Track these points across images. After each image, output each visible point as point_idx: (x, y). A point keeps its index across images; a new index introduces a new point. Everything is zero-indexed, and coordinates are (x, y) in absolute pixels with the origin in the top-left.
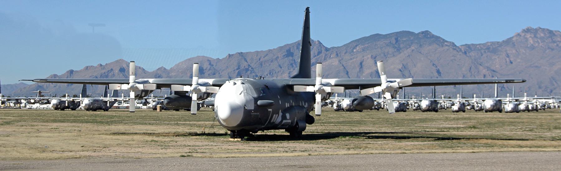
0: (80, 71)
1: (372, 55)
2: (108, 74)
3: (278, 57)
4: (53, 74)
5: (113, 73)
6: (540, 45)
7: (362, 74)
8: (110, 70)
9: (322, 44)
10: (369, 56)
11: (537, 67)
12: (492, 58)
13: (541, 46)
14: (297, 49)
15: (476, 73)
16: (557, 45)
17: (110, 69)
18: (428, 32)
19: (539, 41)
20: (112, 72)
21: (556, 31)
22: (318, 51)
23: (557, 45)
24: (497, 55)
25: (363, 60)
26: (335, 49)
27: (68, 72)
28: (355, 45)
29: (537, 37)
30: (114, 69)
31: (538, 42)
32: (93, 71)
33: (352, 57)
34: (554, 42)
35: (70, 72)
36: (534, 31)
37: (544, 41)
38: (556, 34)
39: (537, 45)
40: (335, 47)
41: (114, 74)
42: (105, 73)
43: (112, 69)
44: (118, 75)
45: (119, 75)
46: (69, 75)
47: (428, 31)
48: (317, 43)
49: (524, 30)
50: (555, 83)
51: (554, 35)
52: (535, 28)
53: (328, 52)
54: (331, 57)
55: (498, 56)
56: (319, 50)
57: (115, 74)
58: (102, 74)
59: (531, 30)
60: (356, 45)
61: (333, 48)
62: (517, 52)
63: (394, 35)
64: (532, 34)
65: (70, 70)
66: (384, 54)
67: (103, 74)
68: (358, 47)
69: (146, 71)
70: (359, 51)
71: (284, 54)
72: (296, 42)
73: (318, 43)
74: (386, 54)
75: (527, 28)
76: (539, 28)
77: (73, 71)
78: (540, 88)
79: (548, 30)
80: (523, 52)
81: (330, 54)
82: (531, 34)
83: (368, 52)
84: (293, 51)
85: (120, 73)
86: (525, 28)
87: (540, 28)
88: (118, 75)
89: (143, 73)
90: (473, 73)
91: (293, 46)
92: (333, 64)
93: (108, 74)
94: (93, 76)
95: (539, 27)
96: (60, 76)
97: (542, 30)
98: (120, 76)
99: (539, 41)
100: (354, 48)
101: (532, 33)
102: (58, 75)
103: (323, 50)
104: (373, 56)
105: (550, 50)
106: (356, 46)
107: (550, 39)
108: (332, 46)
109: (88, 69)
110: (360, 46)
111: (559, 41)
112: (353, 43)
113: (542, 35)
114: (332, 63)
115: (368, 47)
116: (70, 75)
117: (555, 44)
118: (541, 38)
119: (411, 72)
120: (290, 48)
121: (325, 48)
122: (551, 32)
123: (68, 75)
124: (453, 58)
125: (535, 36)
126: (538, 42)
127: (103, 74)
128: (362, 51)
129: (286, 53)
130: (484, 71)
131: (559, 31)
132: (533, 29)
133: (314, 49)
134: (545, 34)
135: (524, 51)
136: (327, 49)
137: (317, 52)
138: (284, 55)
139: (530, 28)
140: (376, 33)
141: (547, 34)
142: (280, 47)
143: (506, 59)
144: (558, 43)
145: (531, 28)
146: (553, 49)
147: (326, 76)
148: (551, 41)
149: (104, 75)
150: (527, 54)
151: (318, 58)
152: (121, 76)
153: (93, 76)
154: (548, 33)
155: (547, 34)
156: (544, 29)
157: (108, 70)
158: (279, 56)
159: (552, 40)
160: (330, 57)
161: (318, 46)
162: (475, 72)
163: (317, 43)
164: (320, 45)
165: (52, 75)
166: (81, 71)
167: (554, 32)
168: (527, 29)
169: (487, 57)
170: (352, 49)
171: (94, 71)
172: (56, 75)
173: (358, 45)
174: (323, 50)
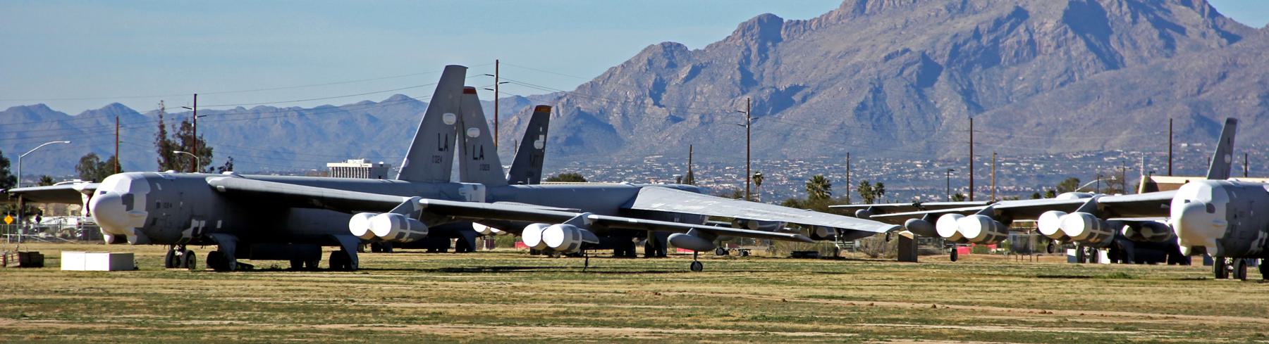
0: (820, 20)
2: (996, 41)
4: (657, 42)
5: (1025, 38)
8: (1009, 18)
17: (1008, 9)
20: (1022, 29)
27: (745, 29)
30: (1031, 9)
32: (900, 22)
35: (756, 30)
41: (1031, 42)
42: (977, 34)
43: (1020, 15)
44: (1058, 47)
45: (1062, 50)
46: (754, 49)
57: (1036, 37)
58: (961, 40)
65: (760, 19)
67: (965, 43)
69: (1225, 21)
77: (782, 19)
85: (1070, 34)
88: (1058, 47)
89: (1212, 31)
93: (996, 41)
94: (908, 54)
96: (697, 51)
98: (1067, 52)
102: (691, 49)
109: (867, 12)
116: (763, 51)
123: (749, 49)
127: (965, 43)
149: (974, 43)
152: (1074, 54)
153: (906, 50)
157: (994, 13)
165: (650, 47)
166: (822, 23)
171: (905, 26)
172: (679, 45)
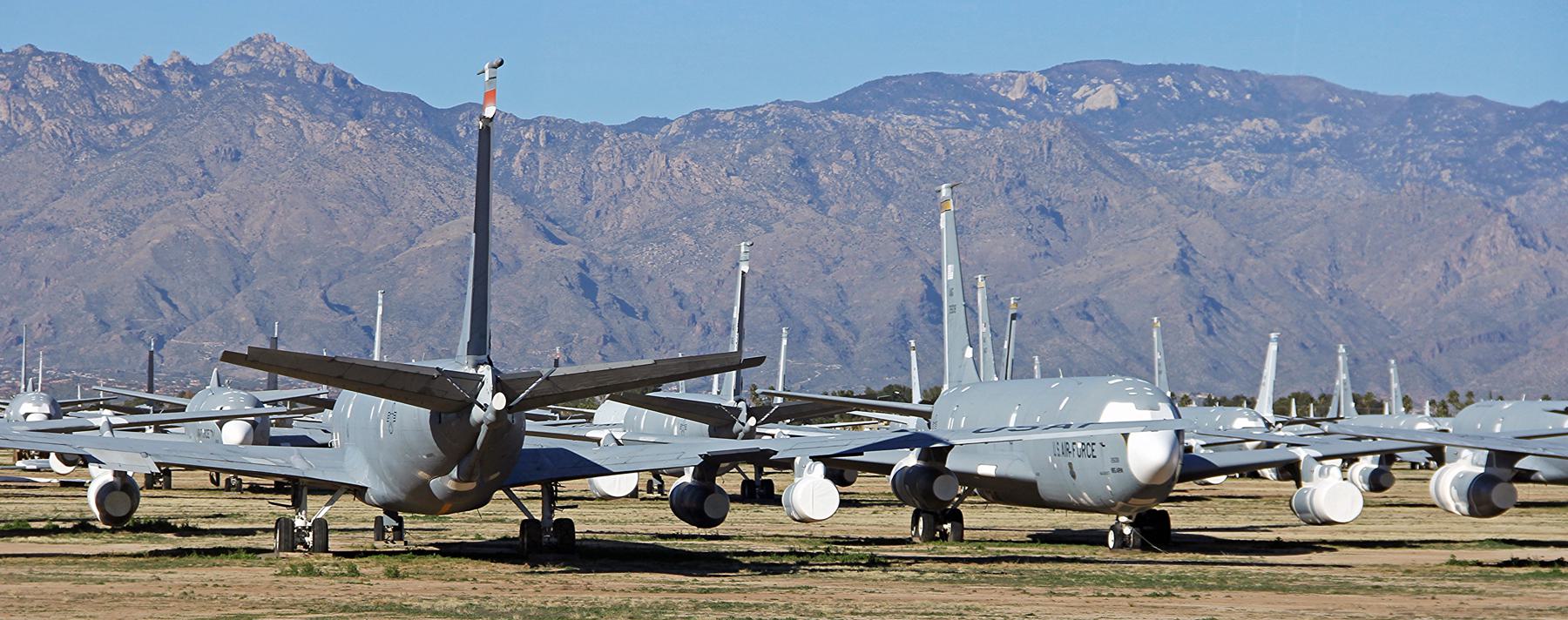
6: (48, 126)
13: (54, 135)
16: (123, 131)
19: (39, 109)
23: (123, 131)
29: (26, 92)
31: (29, 113)
34: (107, 118)
37: (62, 112)
39: (28, 125)
50: (162, 304)
51: (103, 84)
76: (29, 50)
78: (105, 325)
79: (73, 60)
87: (37, 52)
95: (32, 46)
97: (46, 61)
99: (39, 109)
107: (87, 102)
111: (126, 115)
113: (49, 82)
117: (113, 127)
118: (45, 96)
122: (86, 71)
125: (15, 87)
126: (29, 113)
134: (59, 78)
141: (69, 77)
144: (126, 122)
146: (104, 152)
148: (91, 112)
154: (73, 75)
155: (69, 77)
156: (55, 57)
159: (98, 107)
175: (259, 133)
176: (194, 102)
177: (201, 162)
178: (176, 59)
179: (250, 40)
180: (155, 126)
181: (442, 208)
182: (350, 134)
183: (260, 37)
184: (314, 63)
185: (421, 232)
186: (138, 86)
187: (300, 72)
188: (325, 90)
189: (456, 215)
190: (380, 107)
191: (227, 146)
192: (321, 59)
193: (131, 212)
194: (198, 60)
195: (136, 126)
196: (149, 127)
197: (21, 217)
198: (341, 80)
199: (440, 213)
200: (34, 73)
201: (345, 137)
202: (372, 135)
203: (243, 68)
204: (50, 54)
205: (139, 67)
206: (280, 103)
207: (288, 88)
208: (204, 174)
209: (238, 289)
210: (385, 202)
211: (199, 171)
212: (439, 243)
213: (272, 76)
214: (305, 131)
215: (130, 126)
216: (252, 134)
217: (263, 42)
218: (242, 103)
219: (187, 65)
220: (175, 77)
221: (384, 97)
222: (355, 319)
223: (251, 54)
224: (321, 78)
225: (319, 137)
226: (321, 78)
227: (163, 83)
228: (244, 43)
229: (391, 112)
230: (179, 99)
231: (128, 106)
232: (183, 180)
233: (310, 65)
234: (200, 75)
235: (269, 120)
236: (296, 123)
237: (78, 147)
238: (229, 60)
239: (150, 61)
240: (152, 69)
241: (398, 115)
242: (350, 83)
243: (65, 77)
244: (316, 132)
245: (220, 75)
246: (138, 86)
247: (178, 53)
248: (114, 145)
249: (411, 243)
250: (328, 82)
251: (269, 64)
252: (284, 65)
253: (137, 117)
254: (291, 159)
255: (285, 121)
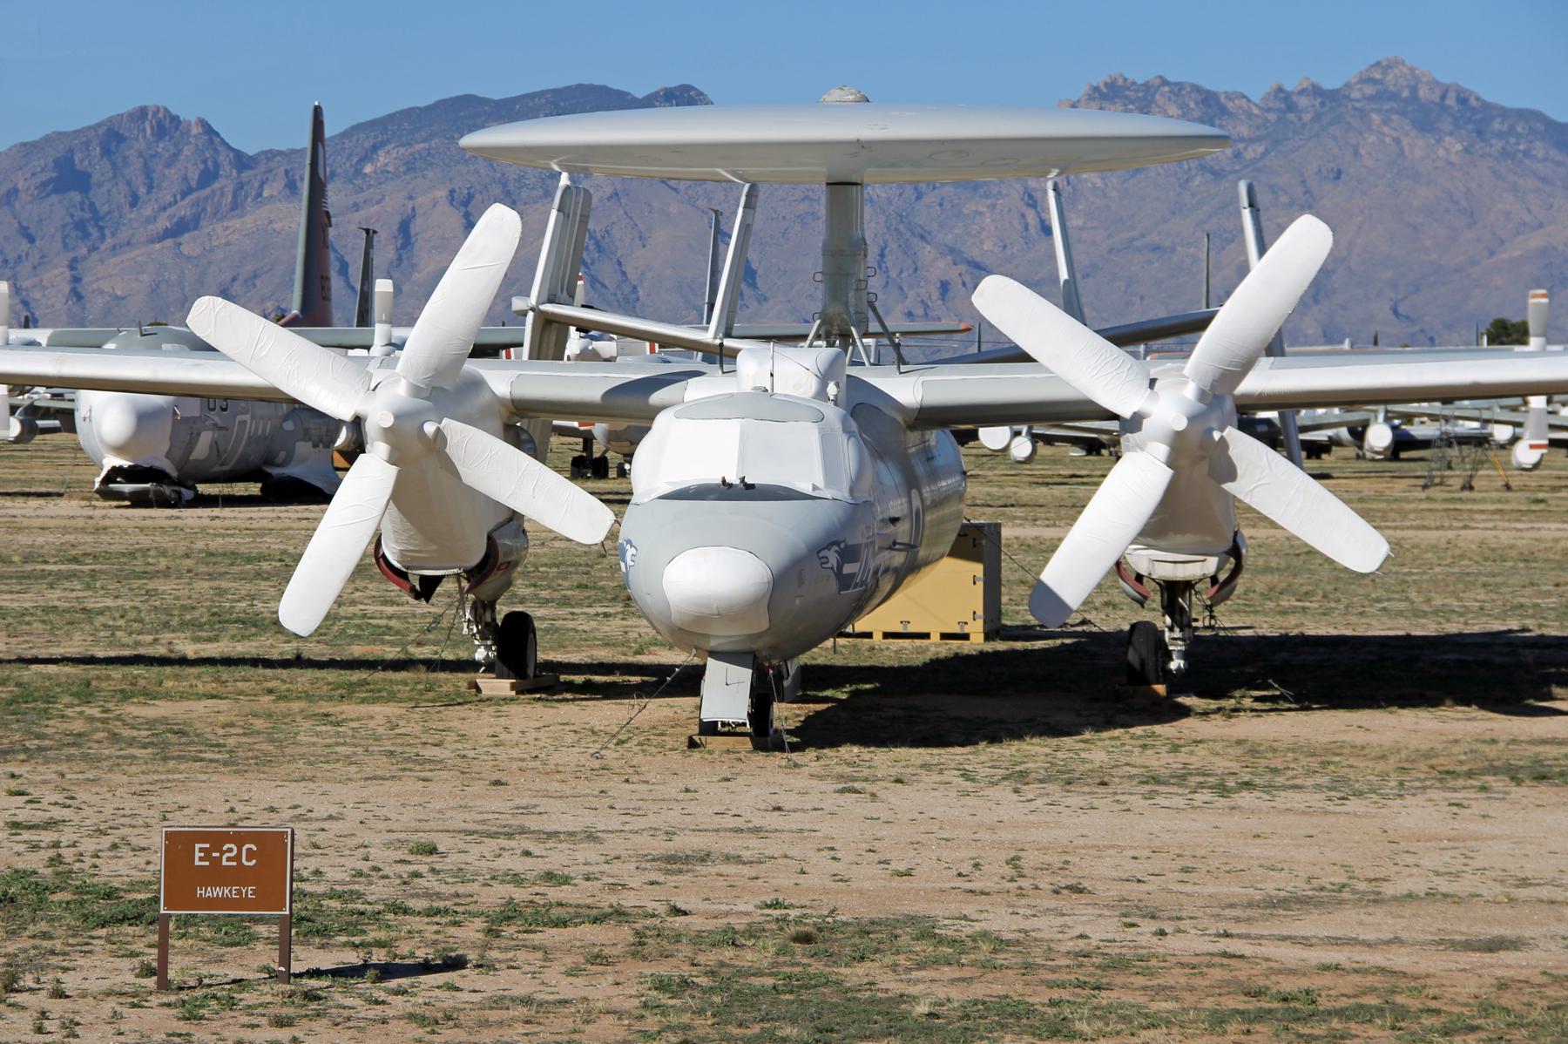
1: (452, 192)
3: (14, 192)
7: (411, 274)
9: (217, 134)
10: (441, 194)
11: (1156, 248)
12: (965, 211)
14: (102, 155)
15: (904, 275)
16: (1237, 155)
18: (692, 93)
21: (1229, 96)
22: (202, 167)
23: (1237, 155)
24: (987, 196)
25: (413, 209)
26: (278, 158)
28: (367, 145)
33: (360, 198)
36: (1140, 94)
38: (1230, 105)
40: (280, 153)
47: (693, 88)
48: (195, 130)
49: (1096, 89)
51: (1223, 110)
52: (1140, 81)
53: (246, 175)
54: (266, 193)
55: (989, 202)
56: (205, 162)
59: (1128, 89)
60: (372, 142)
61: (270, 155)
62: (1069, 184)
63: (543, 101)
64: (1131, 107)
66: (505, 185)
68: (380, 152)
70: (391, 168)
71: (44, 177)
72: (99, 125)
73: (200, 130)
74: (511, 187)
75: (1108, 81)
76: (1158, 82)
79: (1197, 89)
80: (1094, 184)
81: (256, 185)
82: (1125, 105)
83: (430, 174)
84: (86, 162)
86: (1100, 79)
87: (1165, 82)
90: (893, 274)
91: (87, 144)
92: (277, 226)
95: (1161, 77)
100: (367, 157)
101: (1132, 102)
103: (224, 159)
104: (456, 196)
105: (1209, 176)
106: (375, 149)
108: (266, 148)
110: (389, 147)
111: (1242, 140)
112: (362, 136)
114: (271, 222)
115: (429, 154)
117: (1229, 152)
119: (628, 268)
120: (71, 150)
121: (231, 155)
124: (804, 207)
128: (405, 173)
129: (54, 175)
130: (941, 264)
131: (1244, 96)
132: (1134, 83)
133: (182, 157)
135: (1099, 183)
136: (242, 161)
137: (198, 172)
138: (44, 184)
139: (1120, 82)
140: (597, 82)
141: (1192, 105)
142: (24, 145)
143: (1023, 216)
144: (1241, 146)
145: (1125, 80)
147: (246, 281)
150: (1114, 194)
151: (207, 198)
154: (1196, 103)
155: (1192, 105)
156: (1180, 86)
158: (20, 187)
160: (260, 195)
161: (200, 143)
162: (901, 272)
163: (195, 130)
164: (211, 142)
167: (1223, 100)
168: (1106, 84)
169: (941, 205)
170: (355, 160)
173: (382, 144)
174: (224, 159)
175: (1362, 151)
176: (1304, 126)
177: (1303, 182)
178: (1305, 85)
179: (1378, 64)
180: (1266, 149)
181: (1528, 218)
182: (1446, 149)
183: (1388, 60)
184: (1437, 83)
185: (1502, 242)
186: (1256, 111)
187: (1423, 92)
188: (1443, 108)
189: (1541, 226)
190: (1502, 123)
191: (1331, 165)
192: (1445, 79)
193: (1231, 232)
194: (1330, 83)
195: (1250, 149)
196: (1260, 149)
197: (1133, 240)
198: (1463, 100)
199: (1525, 224)
200: (1161, 103)
201: (1441, 153)
202: (1466, 150)
203: (1370, 90)
204: (1176, 84)
205: (1269, 94)
206: (1386, 122)
207: (1410, 108)
208: (1306, 193)
209: (1316, 301)
210: (1472, 213)
211: (1300, 190)
212: (1517, 253)
213: (1394, 96)
214: (1406, 148)
215: (1245, 149)
216: (1356, 153)
217: (1385, 67)
218: (1349, 124)
219: (1316, 91)
220: (1303, 102)
221: (1505, 113)
222: (1422, 331)
223: (1378, 76)
224: (1443, 97)
225: (1418, 153)
226: (1443, 97)
227: (1291, 107)
228: (1373, 66)
229: (1512, 129)
230: (1292, 123)
231: (1244, 131)
232: (1284, 199)
233: (1434, 84)
234: (1328, 98)
235: (1372, 139)
236: (1397, 141)
237: (1194, 172)
238: (1358, 83)
239: (1280, 89)
240: (1282, 95)
241: (1519, 129)
242: (1473, 102)
243: (1188, 106)
244: (1416, 146)
245: (1347, 97)
246: (1256, 111)
247: (1308, 79)
248: (1228, 169)
249: (1492, 254)
250: (1451, 101)
251: (1395, 85)
252: (1408, 86)
253: (1252, 141)
254: (1389, 176)
255: (1387, 140)
